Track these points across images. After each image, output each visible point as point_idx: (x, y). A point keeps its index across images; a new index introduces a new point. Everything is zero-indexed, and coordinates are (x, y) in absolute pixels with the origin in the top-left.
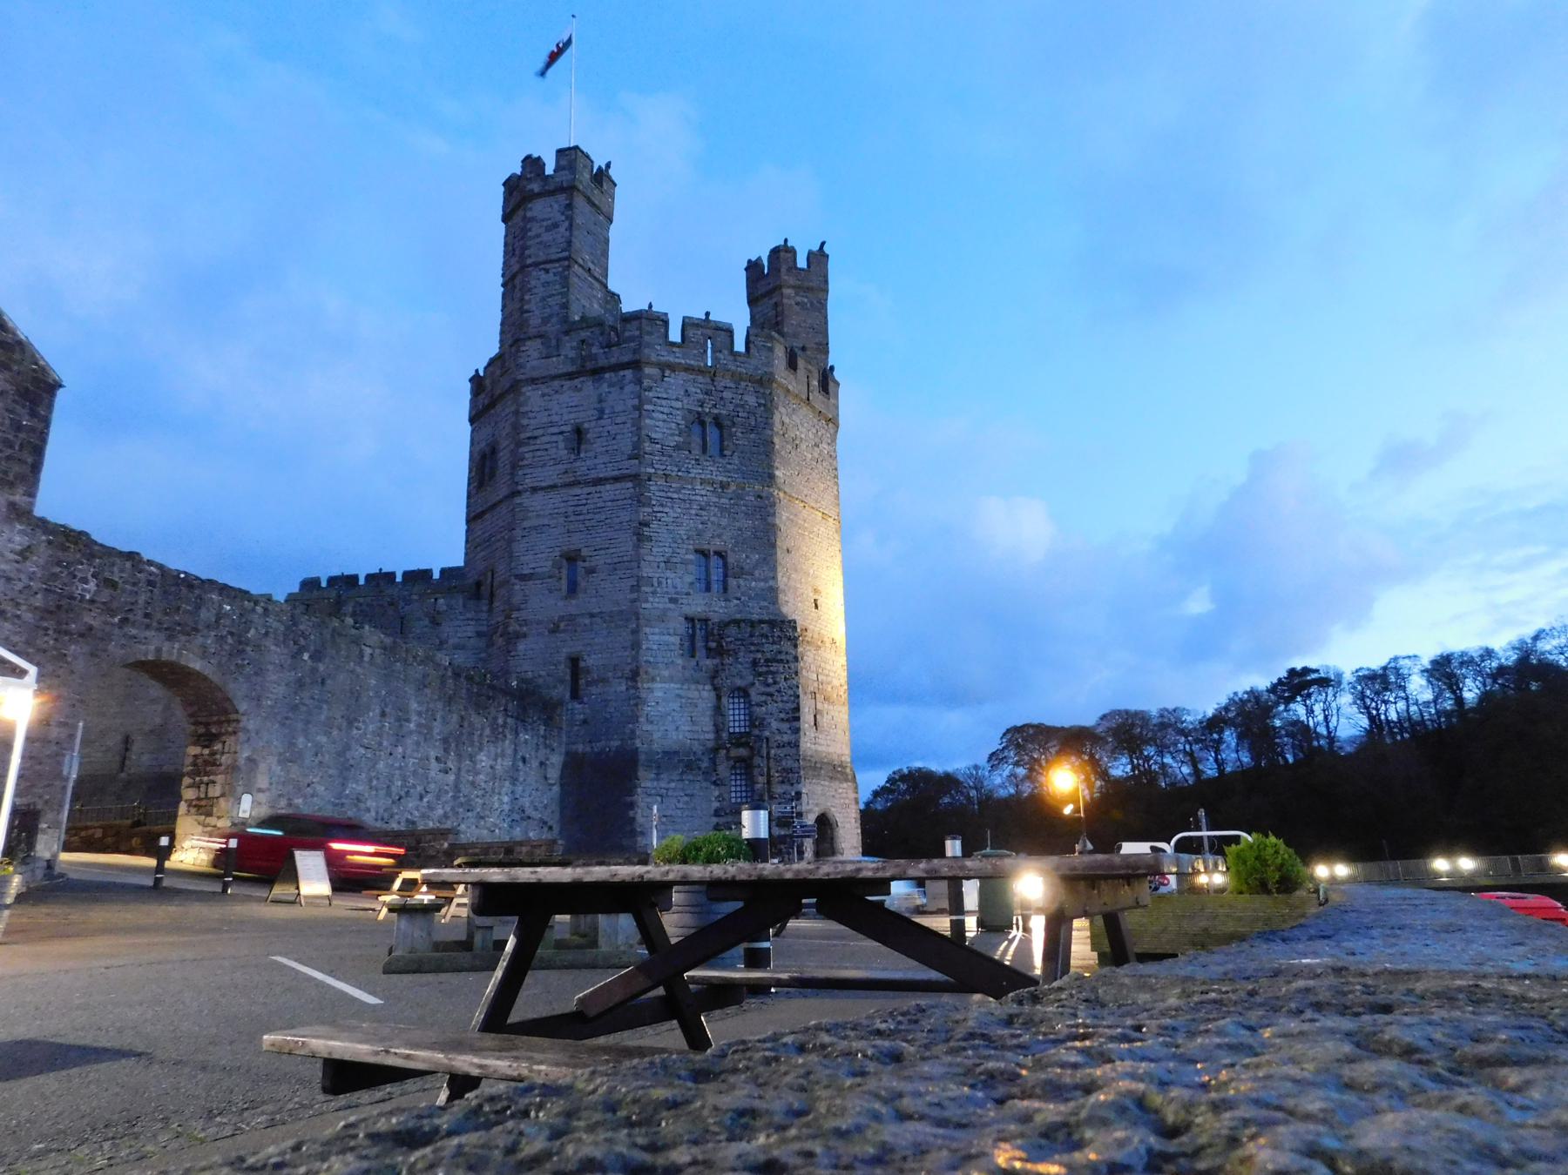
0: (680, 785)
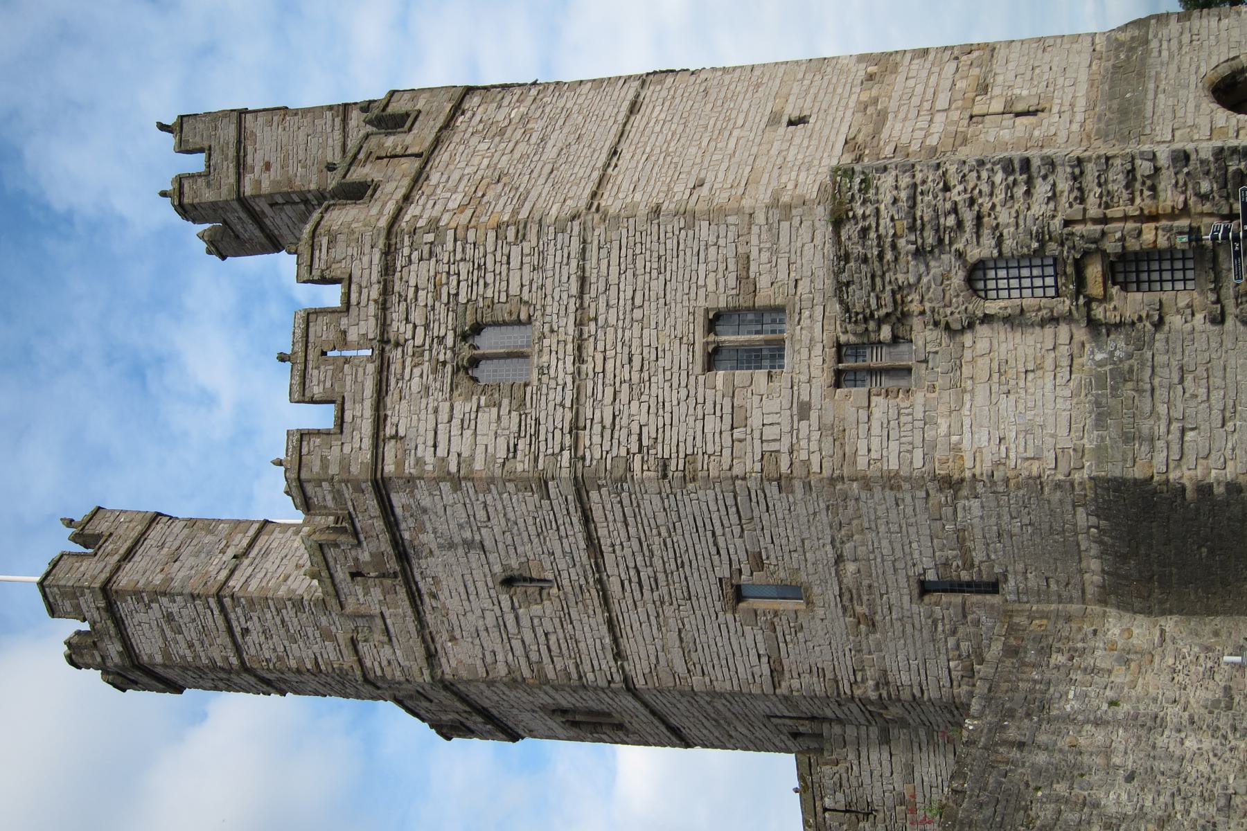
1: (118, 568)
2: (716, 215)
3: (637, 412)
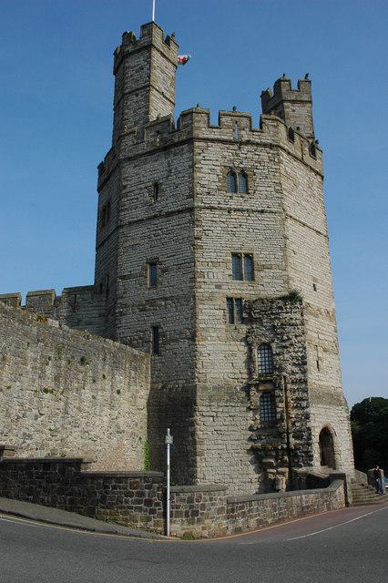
0: (226, 409)
1: (158, 50)
2: (285, 258)
3: (218, 230)
